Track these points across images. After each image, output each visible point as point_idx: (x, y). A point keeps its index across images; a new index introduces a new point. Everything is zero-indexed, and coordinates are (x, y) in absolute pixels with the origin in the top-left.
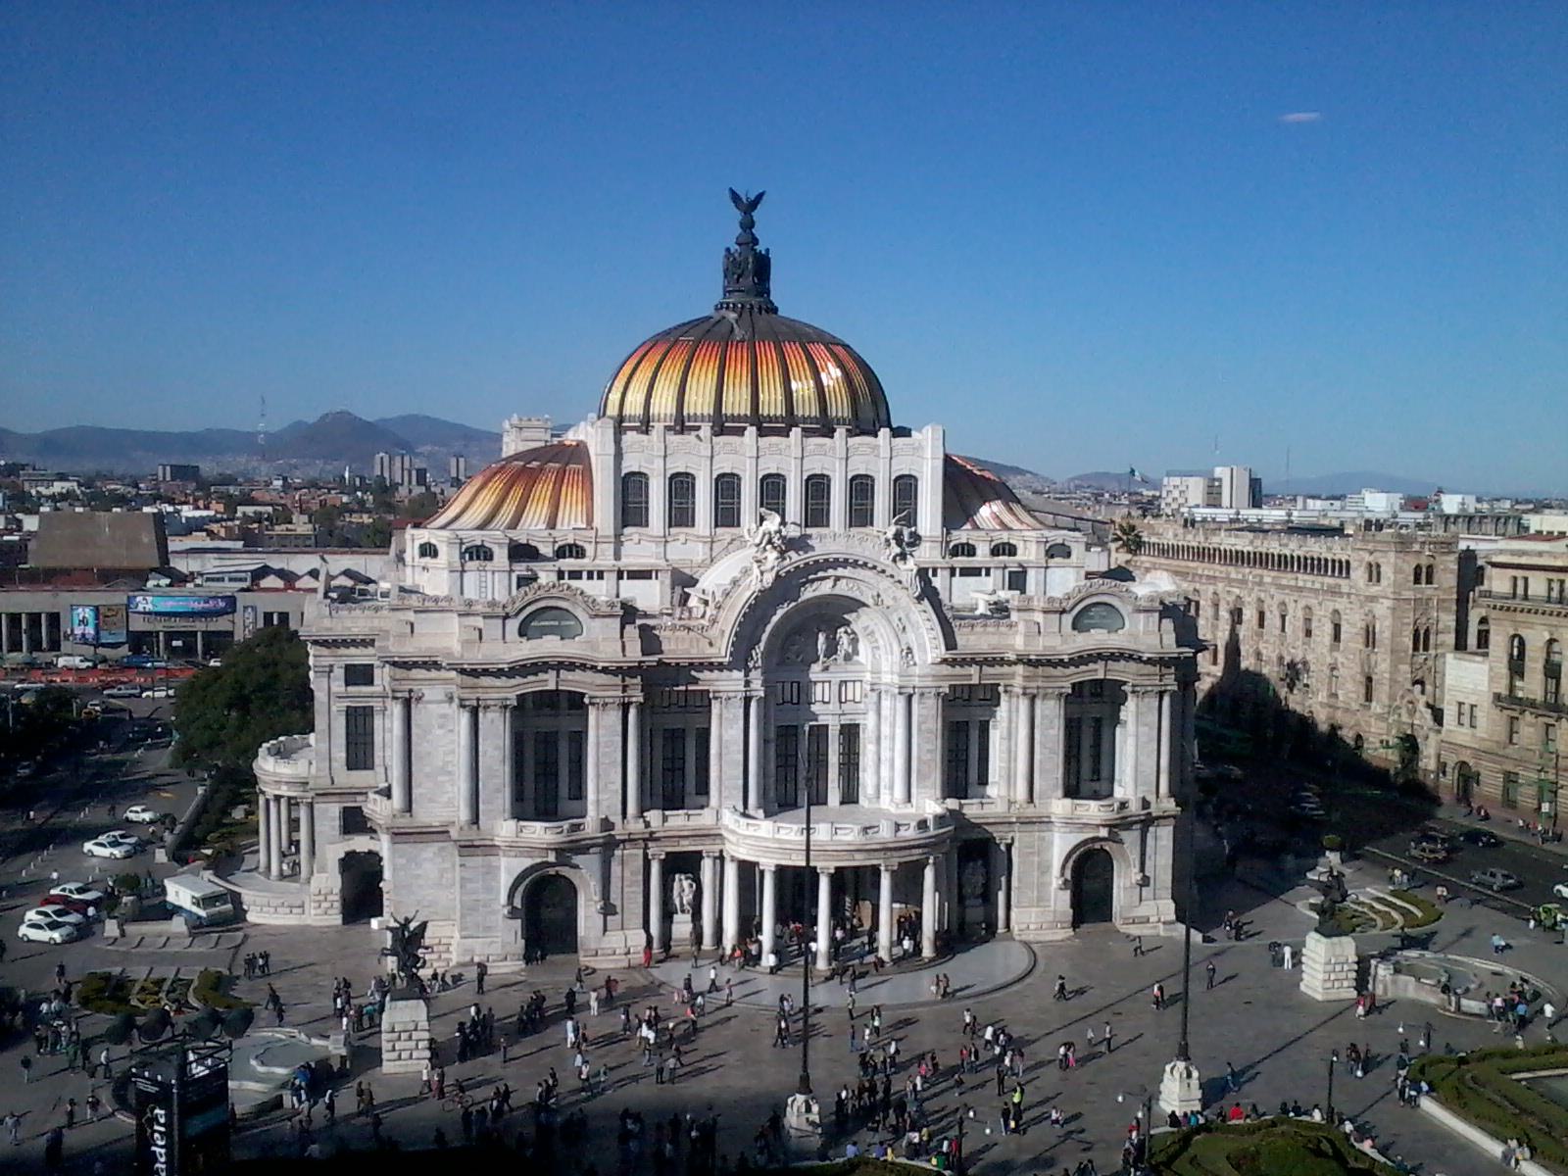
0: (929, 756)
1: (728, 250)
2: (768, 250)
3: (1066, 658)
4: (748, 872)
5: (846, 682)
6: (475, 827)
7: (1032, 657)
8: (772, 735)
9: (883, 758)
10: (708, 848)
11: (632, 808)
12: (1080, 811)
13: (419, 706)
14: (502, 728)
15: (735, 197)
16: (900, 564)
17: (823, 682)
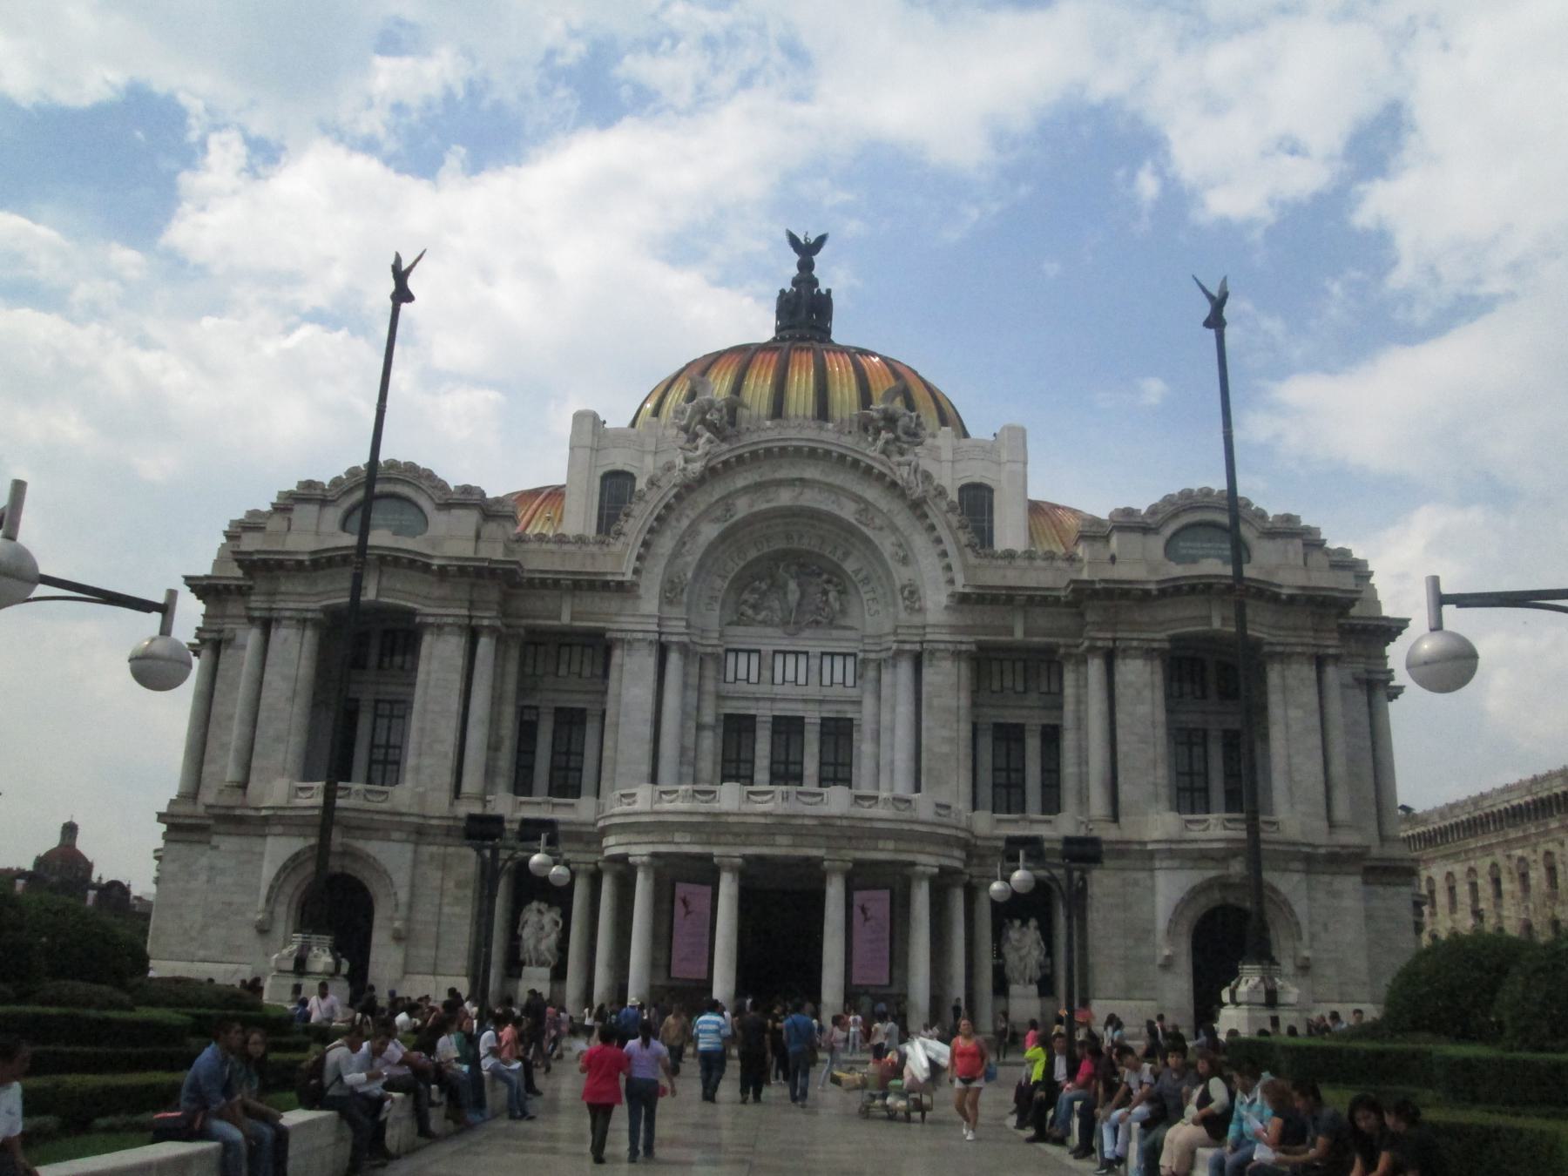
0: (945, 749)
1: (782, 292)
2: (829, 291)
3: (1152, 587)
4: (625, 873)
5: (832, 655)
6: (240, 792)
7: (1098, 586)
8: (708, 717)
9: (882, 763)
10: (581, 857)
11: (471, 783)
12: (1196, 832)
13: (230, 651)
14: (295, 654)
15: (794, 241)
16: (896, 458)
17: (796, 653)
